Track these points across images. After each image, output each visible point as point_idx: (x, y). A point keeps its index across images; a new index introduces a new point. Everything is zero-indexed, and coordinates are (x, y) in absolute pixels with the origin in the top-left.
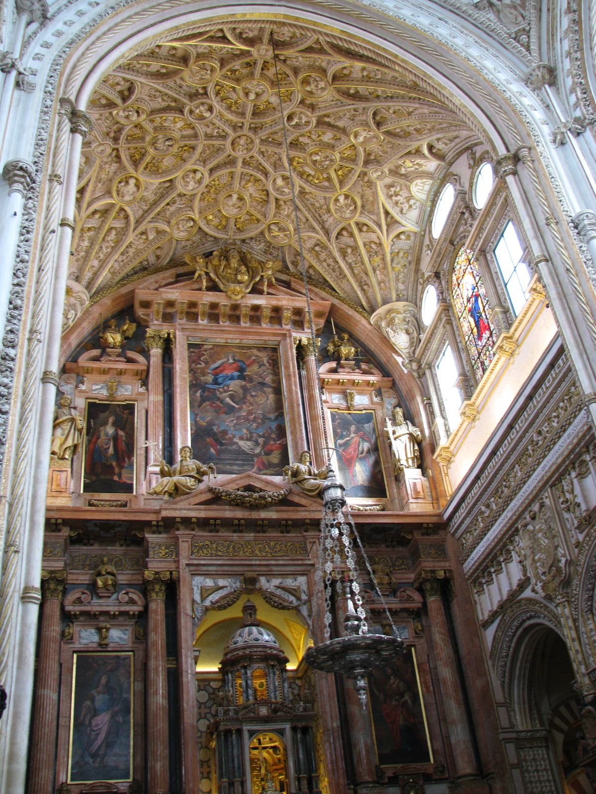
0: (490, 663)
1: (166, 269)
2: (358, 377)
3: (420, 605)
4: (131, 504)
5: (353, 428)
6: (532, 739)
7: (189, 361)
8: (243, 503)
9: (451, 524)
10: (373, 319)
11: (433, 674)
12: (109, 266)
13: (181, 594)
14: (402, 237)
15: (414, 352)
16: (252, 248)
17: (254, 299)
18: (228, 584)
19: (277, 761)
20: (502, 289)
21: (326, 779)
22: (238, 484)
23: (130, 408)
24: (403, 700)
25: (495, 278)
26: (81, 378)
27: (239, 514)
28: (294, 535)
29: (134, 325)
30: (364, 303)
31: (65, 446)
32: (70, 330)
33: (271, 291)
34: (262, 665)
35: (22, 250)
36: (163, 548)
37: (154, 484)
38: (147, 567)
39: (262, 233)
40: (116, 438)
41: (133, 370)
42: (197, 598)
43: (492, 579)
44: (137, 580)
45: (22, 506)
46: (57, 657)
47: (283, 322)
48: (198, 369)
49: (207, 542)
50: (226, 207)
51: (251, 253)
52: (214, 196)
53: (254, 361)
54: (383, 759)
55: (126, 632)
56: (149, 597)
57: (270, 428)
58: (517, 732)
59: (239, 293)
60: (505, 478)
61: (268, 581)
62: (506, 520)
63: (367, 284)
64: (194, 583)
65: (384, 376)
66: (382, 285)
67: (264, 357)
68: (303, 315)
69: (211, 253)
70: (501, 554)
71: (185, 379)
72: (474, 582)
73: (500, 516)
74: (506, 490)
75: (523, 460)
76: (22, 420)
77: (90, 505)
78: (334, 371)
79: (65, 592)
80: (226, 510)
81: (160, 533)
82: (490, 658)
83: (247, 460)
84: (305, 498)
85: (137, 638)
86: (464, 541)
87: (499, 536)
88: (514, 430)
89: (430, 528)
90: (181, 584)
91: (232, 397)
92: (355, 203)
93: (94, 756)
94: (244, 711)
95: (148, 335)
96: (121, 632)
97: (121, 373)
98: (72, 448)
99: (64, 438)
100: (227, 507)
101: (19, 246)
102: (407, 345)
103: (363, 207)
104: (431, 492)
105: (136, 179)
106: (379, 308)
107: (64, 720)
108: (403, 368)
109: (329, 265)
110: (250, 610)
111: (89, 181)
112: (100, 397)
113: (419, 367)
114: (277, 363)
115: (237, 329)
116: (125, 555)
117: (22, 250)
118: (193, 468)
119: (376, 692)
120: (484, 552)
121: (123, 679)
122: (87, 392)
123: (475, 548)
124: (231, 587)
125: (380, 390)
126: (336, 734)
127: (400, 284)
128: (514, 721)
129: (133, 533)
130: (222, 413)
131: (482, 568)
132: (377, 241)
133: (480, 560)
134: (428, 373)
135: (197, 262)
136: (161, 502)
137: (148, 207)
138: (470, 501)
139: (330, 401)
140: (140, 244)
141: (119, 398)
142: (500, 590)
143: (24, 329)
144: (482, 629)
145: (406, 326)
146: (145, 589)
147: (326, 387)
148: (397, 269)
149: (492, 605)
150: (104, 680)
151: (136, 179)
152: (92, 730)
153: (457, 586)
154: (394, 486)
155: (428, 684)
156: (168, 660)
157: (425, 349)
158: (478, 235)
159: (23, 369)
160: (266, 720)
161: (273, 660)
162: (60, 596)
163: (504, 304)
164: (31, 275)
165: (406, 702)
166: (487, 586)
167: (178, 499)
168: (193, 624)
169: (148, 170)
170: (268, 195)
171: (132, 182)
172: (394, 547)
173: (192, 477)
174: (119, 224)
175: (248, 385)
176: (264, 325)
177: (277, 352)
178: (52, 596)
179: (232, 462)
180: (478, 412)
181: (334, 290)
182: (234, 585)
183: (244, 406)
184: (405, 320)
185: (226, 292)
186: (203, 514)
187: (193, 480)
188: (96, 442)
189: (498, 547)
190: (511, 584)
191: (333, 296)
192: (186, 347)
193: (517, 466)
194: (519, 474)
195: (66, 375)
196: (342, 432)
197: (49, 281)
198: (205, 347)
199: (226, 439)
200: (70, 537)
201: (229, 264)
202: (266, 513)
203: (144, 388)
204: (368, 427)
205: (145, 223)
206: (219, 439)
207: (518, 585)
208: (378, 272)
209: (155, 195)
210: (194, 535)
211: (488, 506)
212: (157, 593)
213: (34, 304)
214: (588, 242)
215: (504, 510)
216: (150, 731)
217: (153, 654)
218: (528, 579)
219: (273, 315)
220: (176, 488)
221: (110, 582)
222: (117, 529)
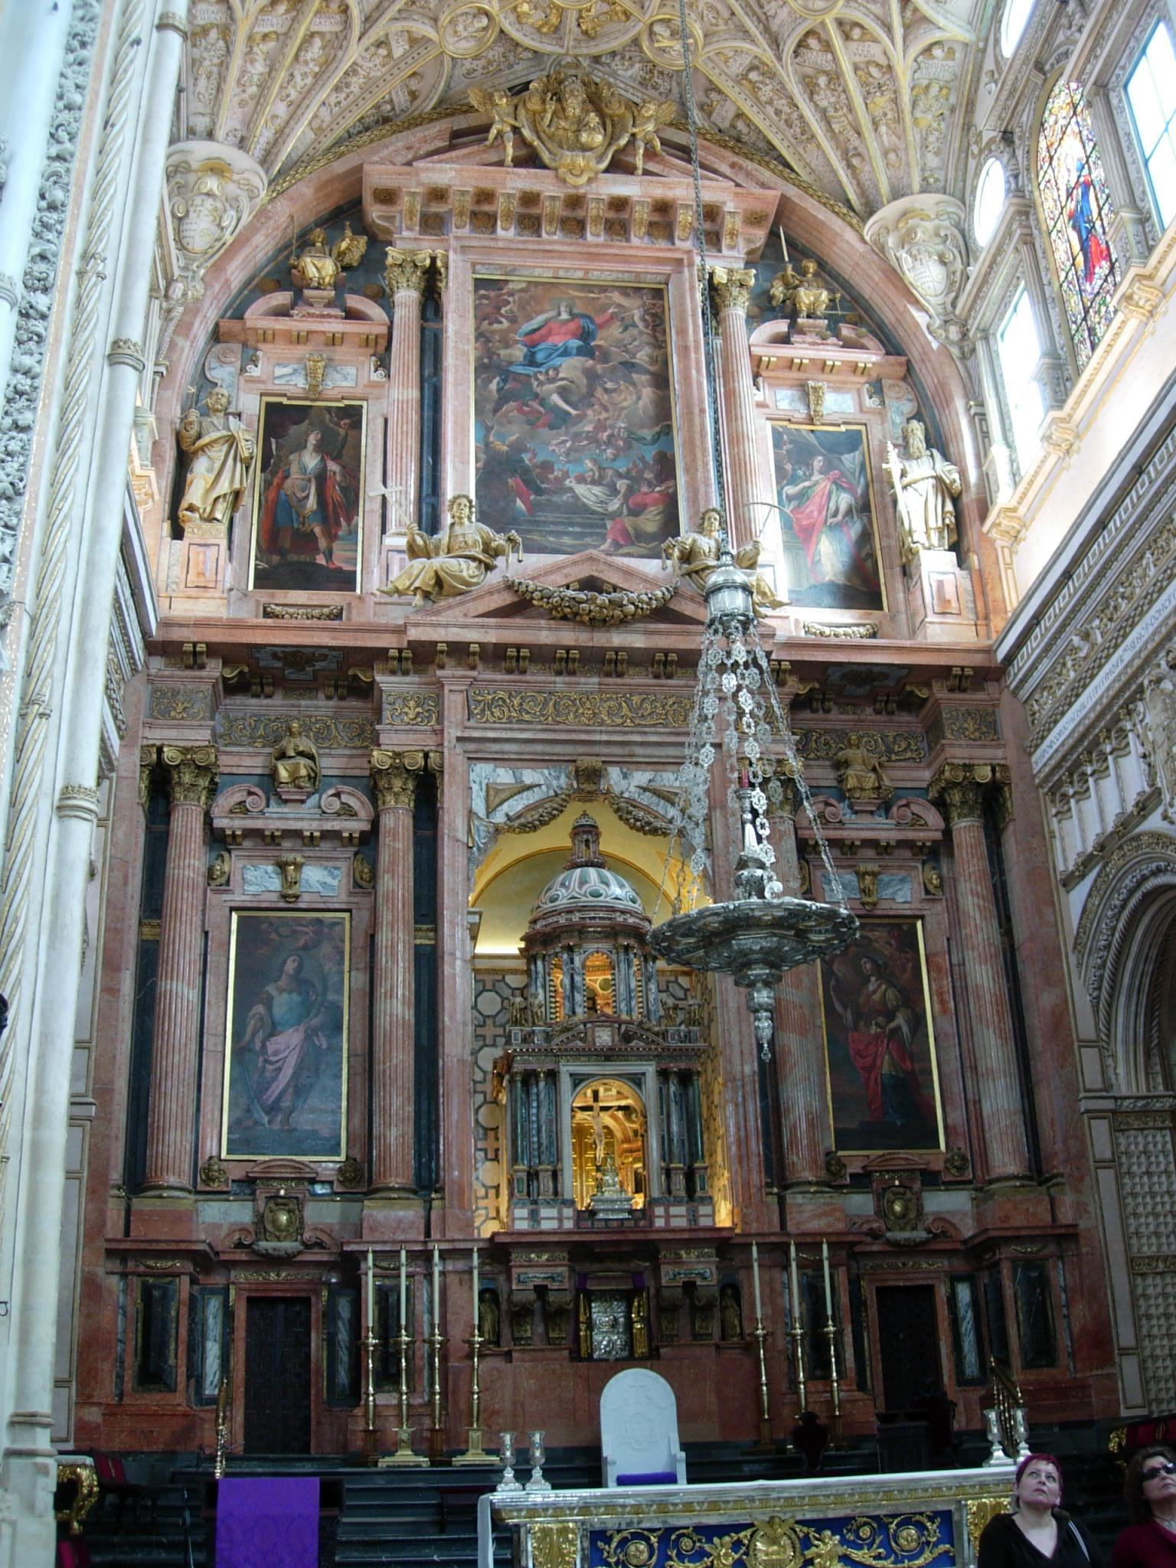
0: (1073, 959)
1: (432, 120)
2: (833, 354)
3: (938, 835)
5: (818, 462)
6: (1144, 1112)
7: (476, 317)
8: (576, 614)
9: (1012, 670)
10: (869, 229)
11: (956, 976)
12: (309, 115)
13: (446, 799)
14: (937, 52)
15: (954, 304)
16: (614, 74)
17: (615, 183)
18: (543, 781)
19: (631, 1134)
20: (1138, 171)
21: (726, 1174)
22: (566, 576)
23: (352, 415)
24: (892, 1025)
25: (1124, 145)
26: (251, 352)
27: (568, 636)
28: (682, 682)
31: (214, 495)
32: (228, 251)
33: (652, 167)
34: (605, 946)
35: (69, 85)
36: (412, 704)
37: (395, 572)
39: (636, 42)
40: (321, 477)
41: (359, 334)
42: (479, 806)
43: (1088, 789)
44: (362, 770)
45: (58, 622)
46: (197, 920)
47: (677, 233)
48: (493, 332)
49: (501, 694)
51: (610, 86)
53: (613, 317)
54: (844, 1139)
55: (336, 872)
56: (380, 802)
57: (642, 459)
58: (1116, 1098)
59: (582, 172)
60: (1123, 577)
61: (625, 777)
62: (1121, 666)
63: (859, 155)
64: (473, 776)
65: (888, 353)
66: (892, 156)
68: (719, 219)
69: (525, 86)
70: (1108, 737)
71: (465, 353)
72: (1053, 791)
73: (1108, 657)
74: (1124, 605)
75: (1161, 542)
76: (61, 445)
77: (267, 614)
78: (784, 340)
79: (213, 791)
80: (540, 629)
81: (406, 673)
82: (1075, 948)
83: (592, 526)
85: (356, 884)
86: (1036, 707)
87: (1105, 701)
88: (1145, 477)
89: (967, 677)
90: (446, 777)
91: (563, 392)
93: (272, 1109)
94: (563, 1037)
95: (389, 261)
96: (325, 873)
97: (333, 340)
98: (230, 498)
99: (212, 476)
100: (543, 622)
101: (62, 75)
102: (940, 287)
104: (975, 602)
106: (883, 206)
107: (212, 1040)
108: (929, 337)
109: (778, 113)
110: (587, 832)
112: (291, 390)
113: (964, 335)
114: (663, 321)
115: (579, 249)
116: (336, 717)
117: (69, 85)
118: (475, 541)
119: (839, 1008)
120: (1073, 731)
121: (329, 966)
123: (1056, 722)
124: (548, 787)
125: (879, 381)
126: (748, 1088)
127: (930, 156)
128: (1113, 1077)
129: (350, 672)
130: (543, 426)
131: (1068, 764)
132: (883, 62)
133: (1066, 748)
135: (494, 105)
136: (410, 609)
138: (1050, 623)
140: (373, 66)
141: (329, 393)
142: (1101, 812)
143: (69, 251)
144: (1062, 890)
145: (940, 247)
146: (373, 786)
147: (764, 373)
148: (924, 124)
149: (1084, 841)
150: (290, 966)
152: (266, 1061)
153: (1016, 800)
154: (899, 586)
155: (946, 996)
156: (416, 930)
157: (977, 297)
158: (1092, 50)
159: (66, 335)
160: (608, 1055)
161: (628, 935)
162: (203, 798)
163: (1140, 204)
164: (88, 138)
165: (899, 1028)
166: (1077, 802)
167: (442, 603)
168: (469, 860)
172: (892, 713)
173: (474, 559)
175: (599, 368)
177: (662, 298)
178: (185, 797)
179: (560, 528)
180: (1078, 436)
181: (788, 166)
183: (590, 412)
184: (937, 235)
186: (492, 637)
187: (473, 565)
188: (280, 486)
189: (1102, 724)
190: (1123, 801)
191: (785, 179)
192: (470, 287)
193: (1148, 555)
194: (1152, 571)
195: (220, 346)
196: (794, 470)
197: (127, 148)
198: (511, 286)
199: (549, 481)
200: (225, 679)
201: (564, 110)
202: (623, 636)
203: (381, 371)
204: (850, 460)
205: (383, 21)
206: (535, 480)
207: (1137, 805)
208: (883, 129)
210: (475, 679)
211: (1086, 636)
212: (396, 795)
213: (94, 198)
215: (1116, 647)
216: (378, 1068)
217: (385, 916)
218: (1157, 792)
219: (656, 218)
220: (439, 582)
221: (303, 772)
222: (319, 665)
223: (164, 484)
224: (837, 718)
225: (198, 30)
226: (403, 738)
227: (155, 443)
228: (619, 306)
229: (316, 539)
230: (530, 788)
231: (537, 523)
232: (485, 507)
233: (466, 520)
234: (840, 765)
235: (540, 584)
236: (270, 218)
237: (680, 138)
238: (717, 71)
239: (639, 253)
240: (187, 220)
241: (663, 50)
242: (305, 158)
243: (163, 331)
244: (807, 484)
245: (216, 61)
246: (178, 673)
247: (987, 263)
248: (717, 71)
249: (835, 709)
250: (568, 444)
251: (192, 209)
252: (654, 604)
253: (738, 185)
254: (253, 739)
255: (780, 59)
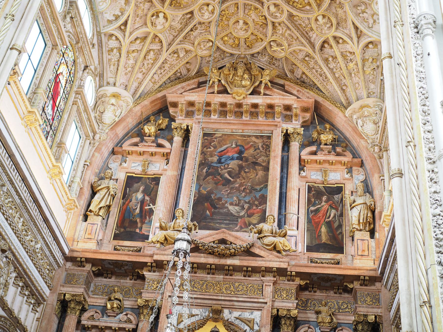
1: (193, 78)
2: (332, 158)
4: (144, 249)
5: (324, 198)
7: (202, 146)
10: (348, 112)
12: (149, 77)
14: (370, 46)
16: (259, 61)
17: (253, 98)
22: (213, 238)
23: (156, 180)
26: (125, 158)
27: (211, 260)
29: (167, 120)
30: (343, 100)
32: (116, 123)
33: (267, 92)
36: (156, 283)
38: (141, 298)
40: (143, 202)
41: (161, 152)
48: (207, 152)
50: (236, 31)
52: (226, 23)
53: (251, 146)
57: (255, 197)
61: (230, 313)
67: (260, 143)
77: (115, 249)
79: (83, 310)
80: (201, 257)
81: (154, 272)
84: (264, 251)
89: (367, 280)
90: (162, 310)
91: (230, 173)
92: (331, 22)
95: (172, 127)
97: (152, 154)
99: (99, 200)
100: (202, 255)
103: (338, 24)
105: (164, 13)
109: (317, 71)
111: (129, 16)
113: (381, 150)
114: (269, 147)
115: (240, 122)
116: (133, 286)
122: (127, 169)
124: (201, 316)
125: (351, 168)
129: (136, 271)
132: (351, 51)
134: (385, 154)
137: (177, 33)
139: (308, 177)
141: (149, 173)
147: (307, 165)
151: (164, 13)
162: (78, 313)
167: (167, 247)
169: (172, 6)
170: (266, 19)
171: (161, 15)
172: (341, 293)
174: (156, 47)
176: (260, 119)
177: (270, 139)
178: (71, 312)
179: (221, 221)
182: (204, 314)
183: (238, 180)
185: (232, 94)
188: (128, 205)
195: (115, 156)
196: (315, 201)
198: (216, 135)
199: (219, 204)
200: (93, 271)
208: (353, 75)
209: (181, 24)
214: (423, 39)
220: (166, 239)
221: (115, 306)
222: (126, 267)
223: (82, 202)
224: (319, 295)
225: (110, 49)
226: (150, 295)
227: (81, 188)
228: (254, 142)
229: (137, 223)
230: (194, 316)
231: (213, 219)
232: (195, 213)
233: (181, 218)
234: (318, 313)
235: (202, 241)
236: (133, 113)
237: (281, 82)
238: (294, 58)
239: (261, 123)
240: (104, 113)
241: (274, 51)
242: (149, 92)
243: (91, 151)
244: (319, 206)
245: (116, 60)
246: (76, 268)
247: (384, 123)
248: (294, 58)
249: (318, 291)
250: (228, 191)
251: (106, 110)
252: (242, 249)
253: (298, 98)
254: (103, 293)
255: (315, 52)
